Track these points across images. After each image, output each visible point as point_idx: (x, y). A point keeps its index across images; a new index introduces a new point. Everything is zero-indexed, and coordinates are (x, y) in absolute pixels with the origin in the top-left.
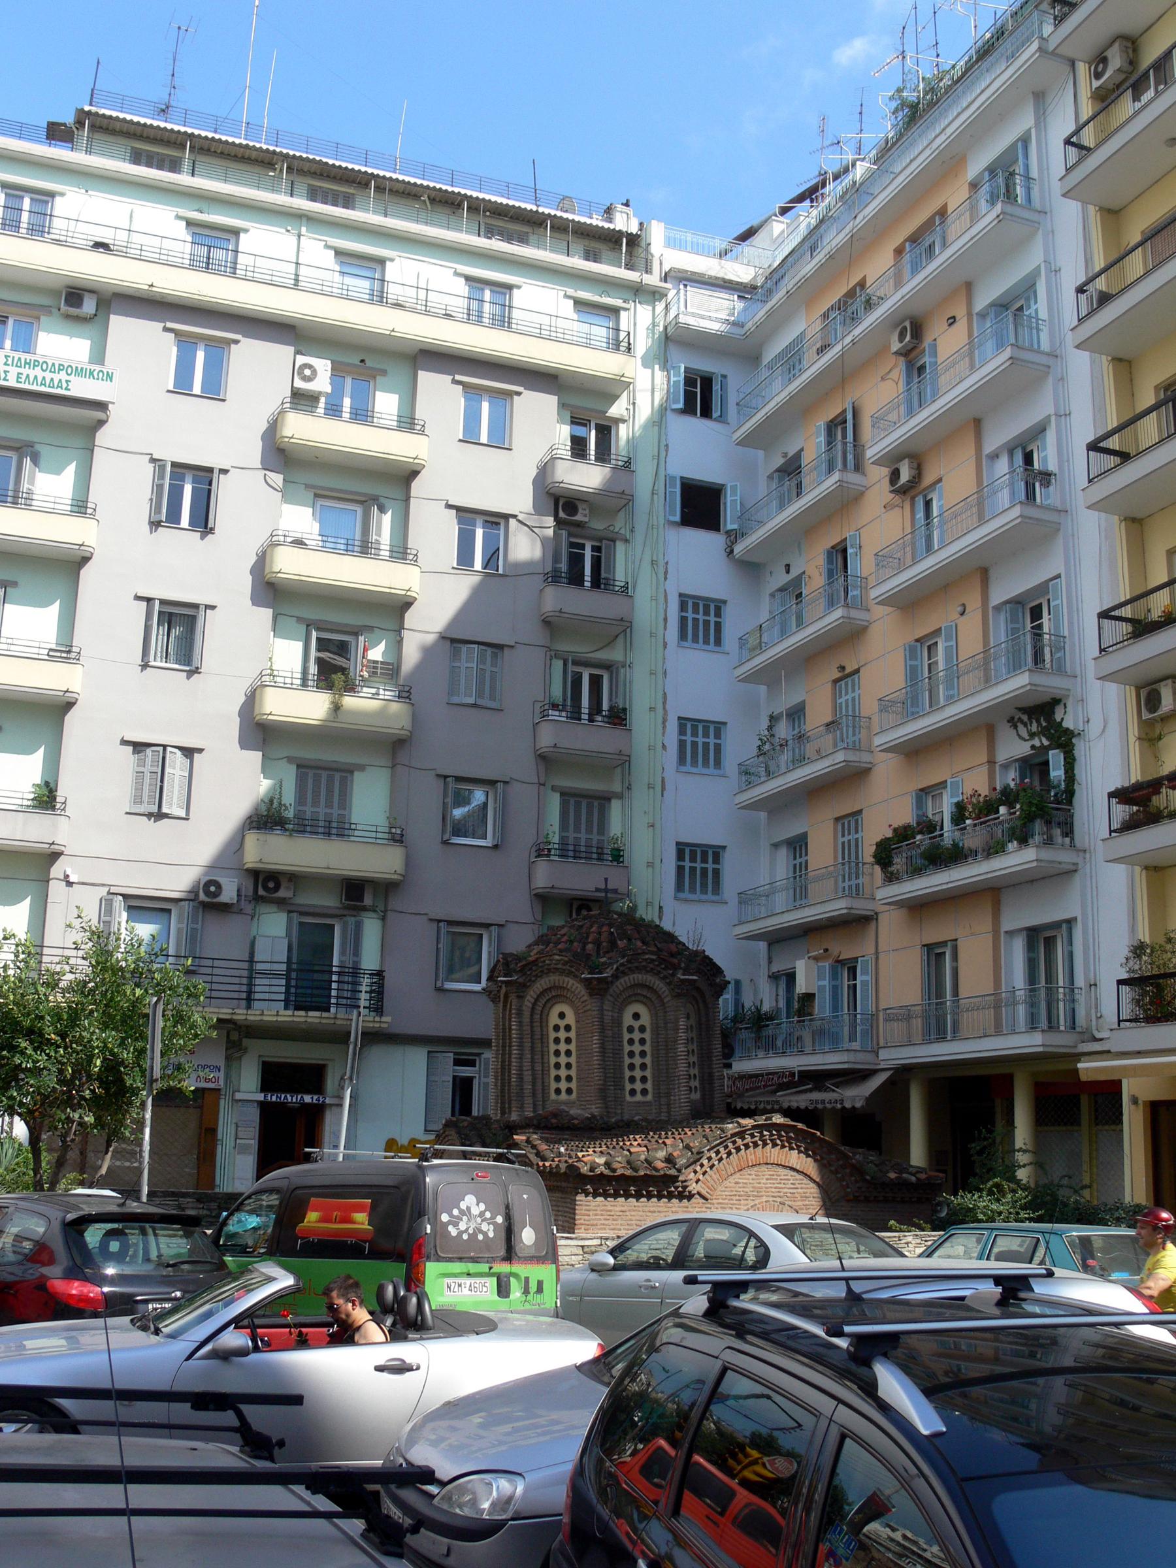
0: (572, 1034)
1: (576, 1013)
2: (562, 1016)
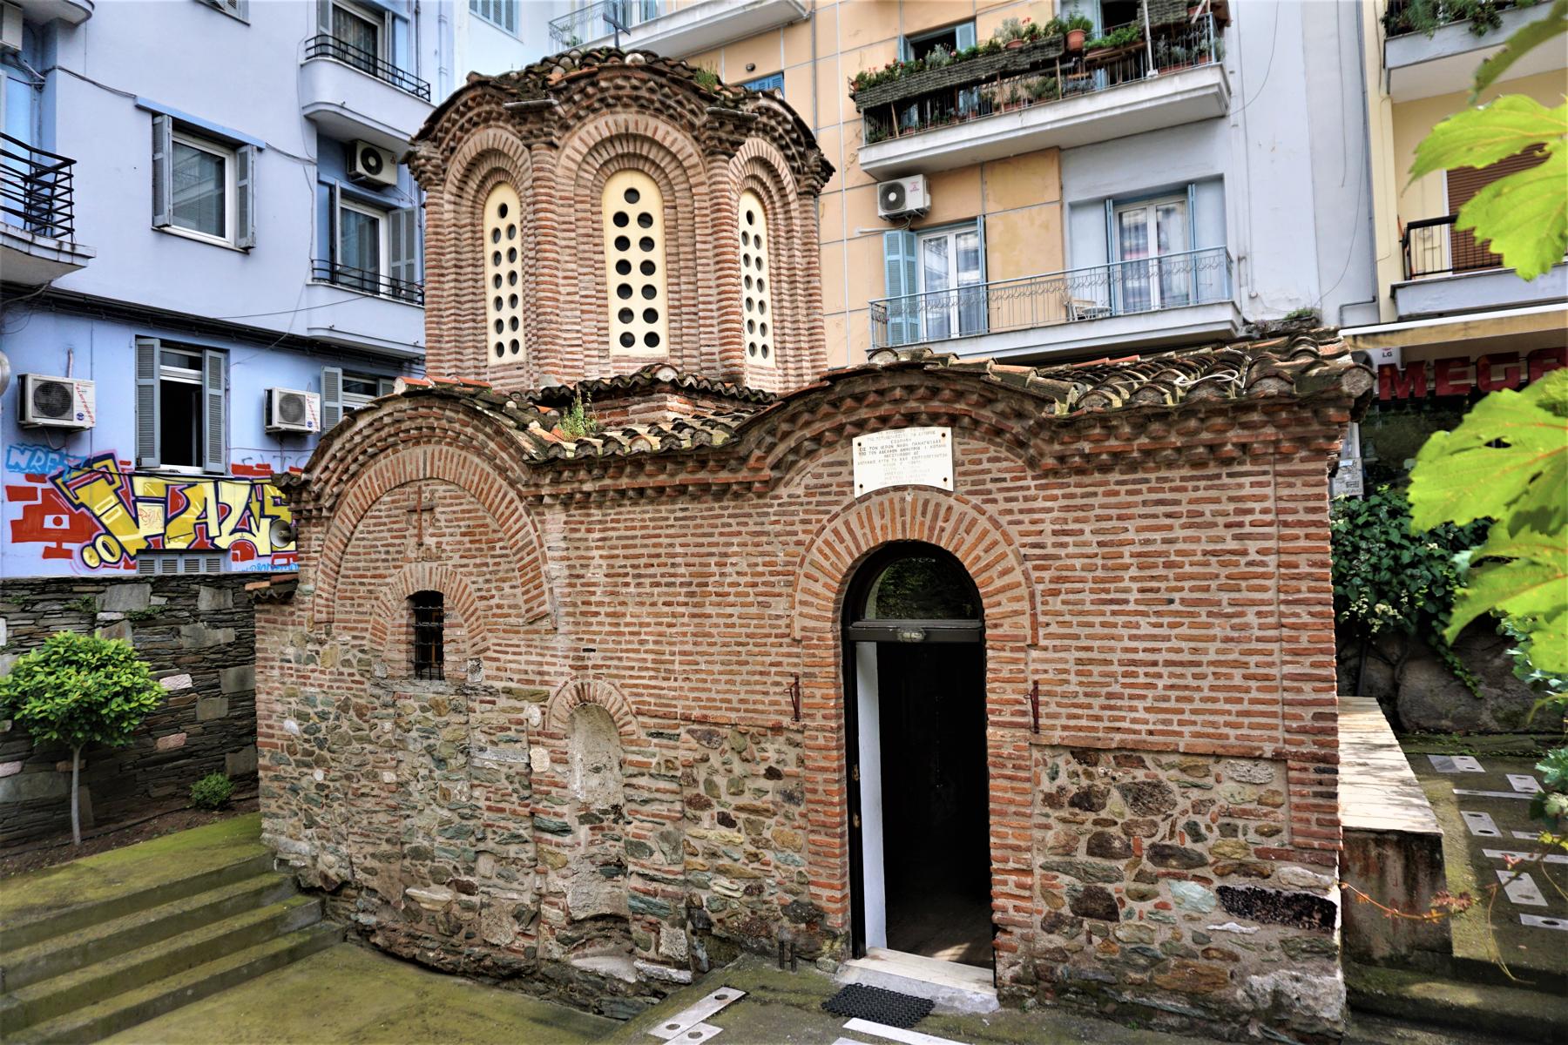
0: (656, 232)
1: (666, 185)
2: (632, 195)
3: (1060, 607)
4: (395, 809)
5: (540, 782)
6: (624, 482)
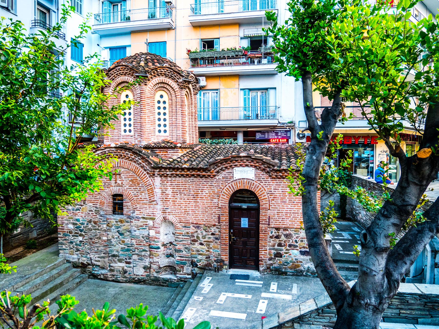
0: (167, 105)
2: (162, 96)
3: (274, 203)
4: (106, 246)
5: (152, 238)
6: (178, 173)
